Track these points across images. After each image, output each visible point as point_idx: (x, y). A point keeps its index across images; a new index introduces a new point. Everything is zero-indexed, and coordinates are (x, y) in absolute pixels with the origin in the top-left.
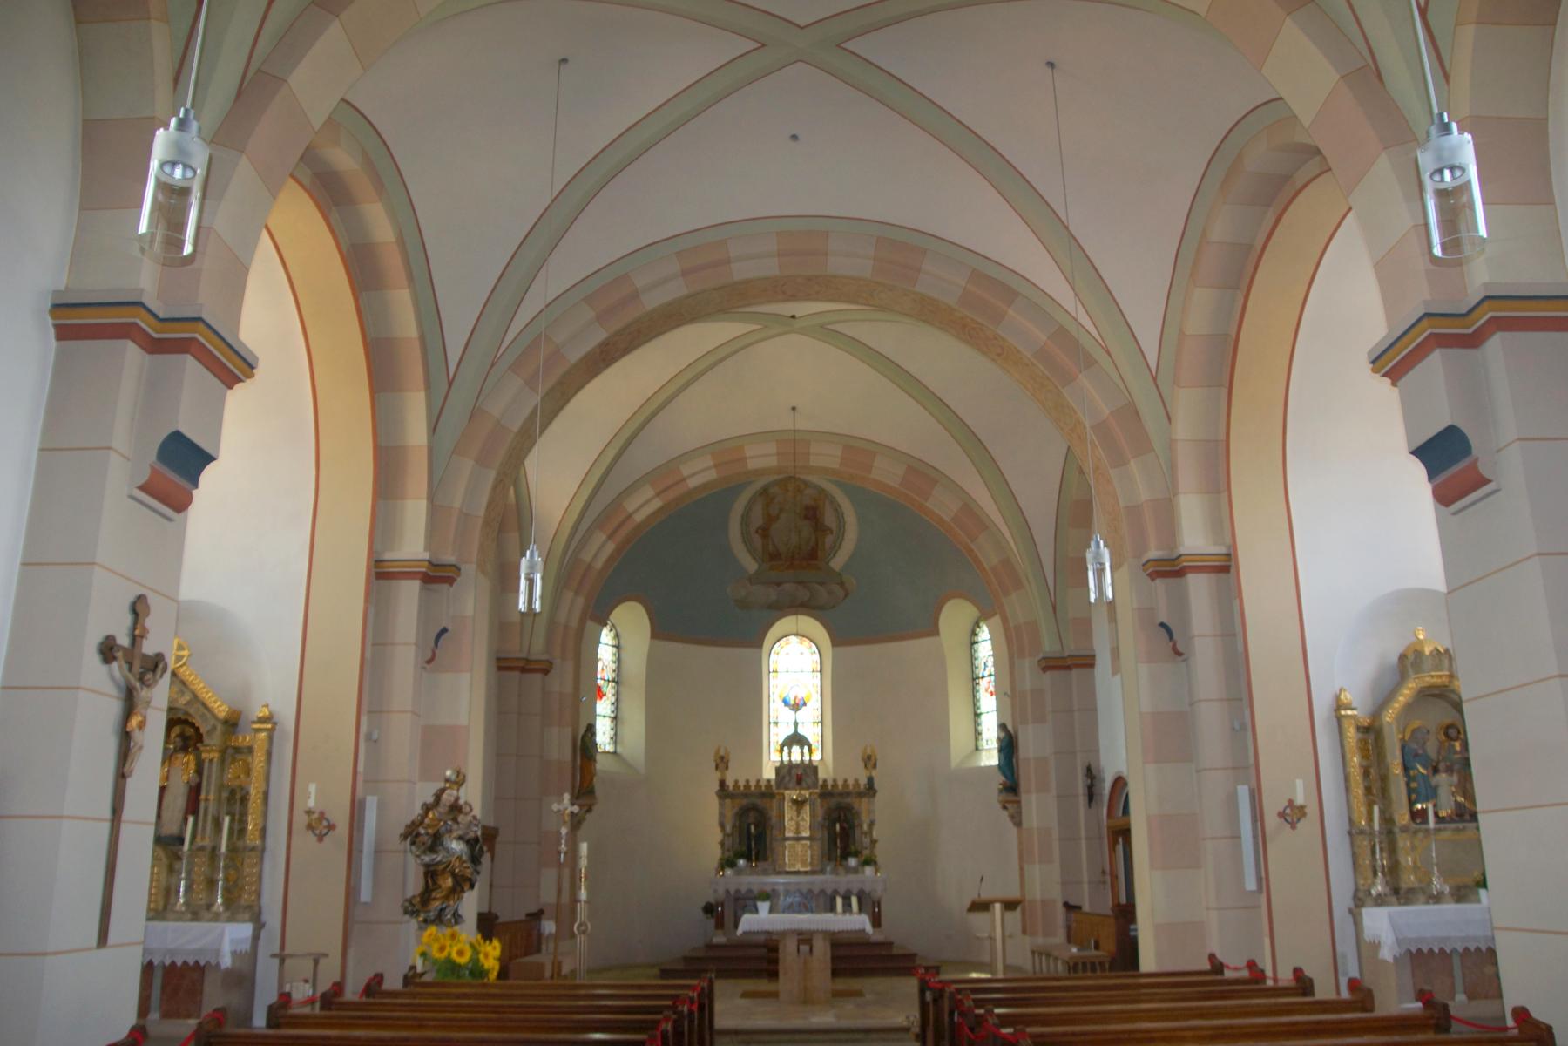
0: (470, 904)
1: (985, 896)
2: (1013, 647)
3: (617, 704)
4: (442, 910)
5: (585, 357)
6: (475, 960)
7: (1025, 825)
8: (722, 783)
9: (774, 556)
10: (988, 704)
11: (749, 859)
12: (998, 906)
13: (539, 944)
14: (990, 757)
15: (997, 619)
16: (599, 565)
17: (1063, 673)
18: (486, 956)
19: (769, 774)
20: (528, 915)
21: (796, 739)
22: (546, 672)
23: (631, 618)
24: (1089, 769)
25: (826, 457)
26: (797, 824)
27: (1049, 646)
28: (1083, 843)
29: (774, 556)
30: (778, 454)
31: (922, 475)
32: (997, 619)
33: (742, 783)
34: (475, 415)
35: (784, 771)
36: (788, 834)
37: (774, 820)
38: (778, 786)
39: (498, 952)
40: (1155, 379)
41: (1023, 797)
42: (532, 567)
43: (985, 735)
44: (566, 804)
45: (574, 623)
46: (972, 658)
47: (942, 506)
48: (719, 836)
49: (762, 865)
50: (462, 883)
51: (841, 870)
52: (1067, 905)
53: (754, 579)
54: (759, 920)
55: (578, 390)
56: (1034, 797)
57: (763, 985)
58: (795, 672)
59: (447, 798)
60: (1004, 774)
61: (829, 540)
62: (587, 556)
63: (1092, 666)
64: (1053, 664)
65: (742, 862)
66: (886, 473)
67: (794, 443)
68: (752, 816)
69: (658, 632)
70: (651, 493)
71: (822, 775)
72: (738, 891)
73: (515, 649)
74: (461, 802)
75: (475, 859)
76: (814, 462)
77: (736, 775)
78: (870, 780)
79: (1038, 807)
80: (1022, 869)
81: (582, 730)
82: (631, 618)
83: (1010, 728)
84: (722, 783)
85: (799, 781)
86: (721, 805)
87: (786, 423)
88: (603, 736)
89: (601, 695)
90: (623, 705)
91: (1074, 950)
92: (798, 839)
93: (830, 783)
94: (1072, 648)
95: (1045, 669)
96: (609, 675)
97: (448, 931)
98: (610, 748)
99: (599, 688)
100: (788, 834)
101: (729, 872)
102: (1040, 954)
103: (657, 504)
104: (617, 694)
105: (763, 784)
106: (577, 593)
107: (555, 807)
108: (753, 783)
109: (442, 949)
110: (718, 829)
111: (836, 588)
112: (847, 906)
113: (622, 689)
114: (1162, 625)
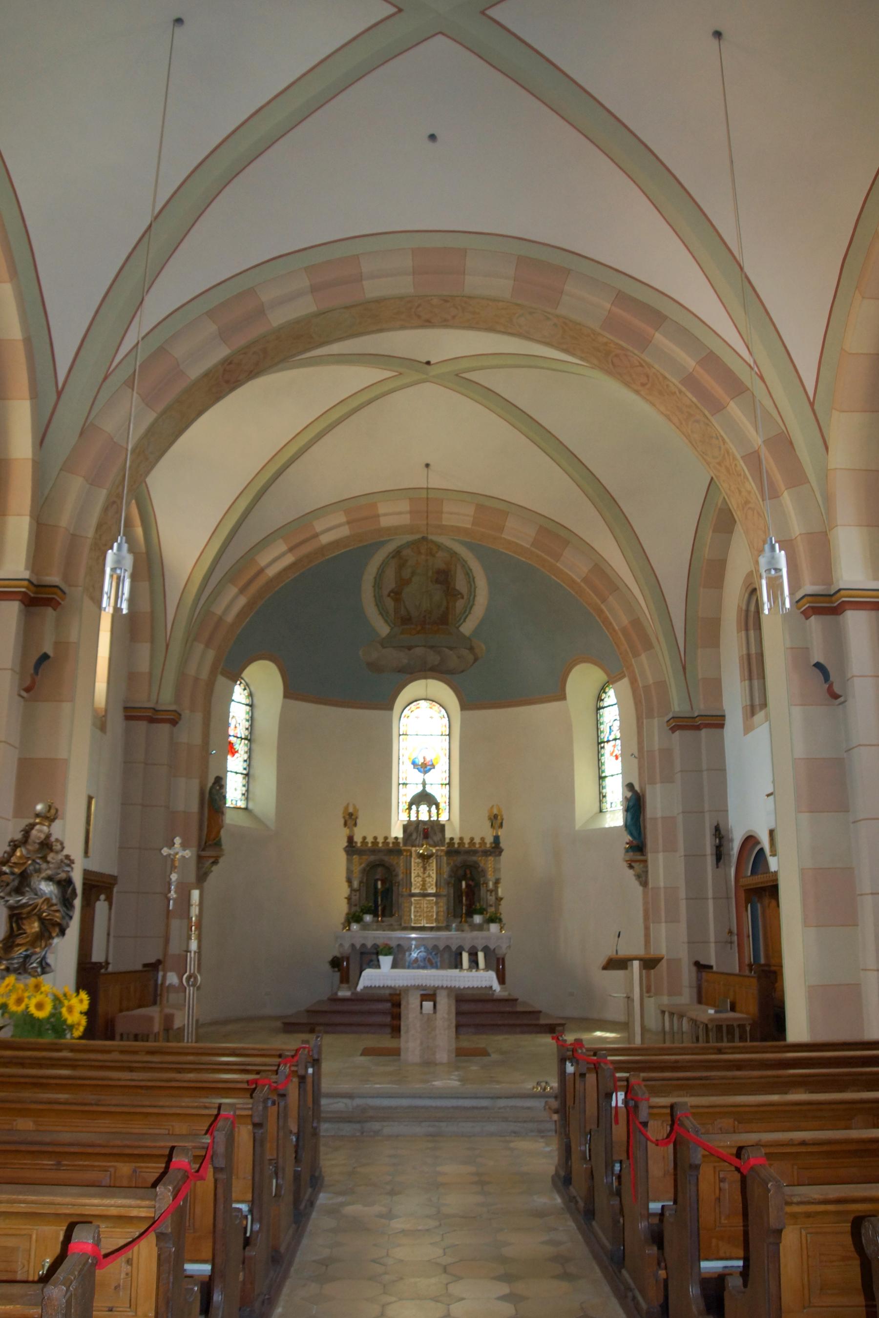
0: (64, 952)
1: (624, 951)
2: (642, 707)
3: (249, 761)
4: (27, 957)
5: (206, 375)
6: (56, 1014)
7: (650, 885)
8: (350, 839)
9: (406, 620)
10: (613, 767)
11: (375, 914)
12: (636, 964)
13: (155, 996)
14: (615, 817)
15: (625, 682)
16: (230, 618)
17: (688, 733)
18: (70, 1010)
19: (397, 832)
20: (145, 965)
21: (424, 798)
22: (174, 722)
23: (264, 676)
24: (717, 829)
25: (459, 516)
26: (424, 879)
27: (678, 706)
28: (711, 903)
29: (406, 620)
30: (411, 512)
31: (554, 536)
32: (625, 682)
33: (370, 840)
34: (86, 431)
35: (411, 829)
37: (401, 876)
38: (405, 844)
39: (85, 1006)
40: (812, 404)
41: (650, 857)
42: (118, 562)
43: (609, 799)
44: (181, 851)
45: (204, 675)
46: (598, 723)
47: (574, 567)
48: (345, 890)
49: (392, 920)
50: (53, 928)
51: (466, 927)
52: (697, 964)
53: (385, 643)
54: (382, 975)
55: (200, 413)
56: (661, 856)
57: (385, 1041)
58: (424, 733)
59: (38, 833)
60: (631, 834)
61: (460, 604)
62: (218, 610)
63: (722, 726)
64: (682, 724)
65: (368, 918)
66: (519, 534)
67: (426, 502)
68: (380, 873)
69: (290, 693)
70: (284, 548)
71: (448, 835)
72: (363, 945)
73: (143, 700)
74: (53, 839)
75: (67, 902)
76: (448, 520)
77: (364, 832)
78: (497, 839)
79: (665, 866)
80: (647, 928)
81: (211, 780)
82: (264, 676)
83: (637, 788)
84: (350, 839)
85: (426, 835)
86: (349, 861)
87: (418, 480)
88: (234, 792)
89: (233, 752)
90: (254, 763)
91: (711, 1011)
93: (456, 841)
94: (701, 707)
95: (673, 729)
96: (242, 731)
97: (32, 981)
98: (242, 804)
99: (231, 745)
100: (415, 890)
101: (355, 927)
102: (673, 1014)
103: (289, 559)
104: (250, 752)
105: (390, 840)
106: (208, 645)
107: (165, 851)
108: (380, 840)
109: (19, 1001)
110: (345, 885)
111: (465, 652)
112: (474, 963)
113: (254, 746)
114: (818, 665)
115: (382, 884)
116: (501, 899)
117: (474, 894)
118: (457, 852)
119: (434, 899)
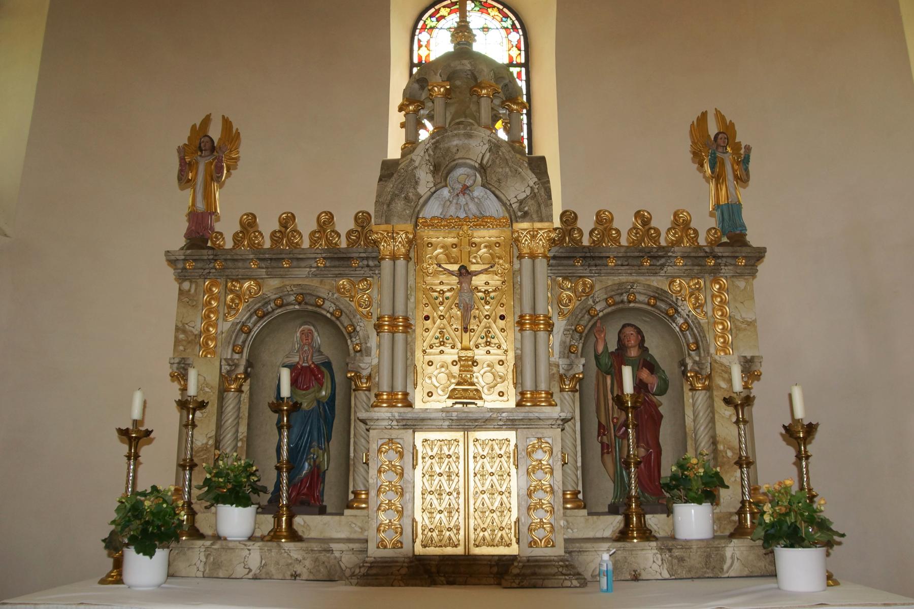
33: (268, 226)
36: (432, 394)
65: (235, 521)
92: (467, 423)
115: (294, 383)
116: (811, 429)
117: (656, 419)
118: (592, 257)
119: (511, 435)
